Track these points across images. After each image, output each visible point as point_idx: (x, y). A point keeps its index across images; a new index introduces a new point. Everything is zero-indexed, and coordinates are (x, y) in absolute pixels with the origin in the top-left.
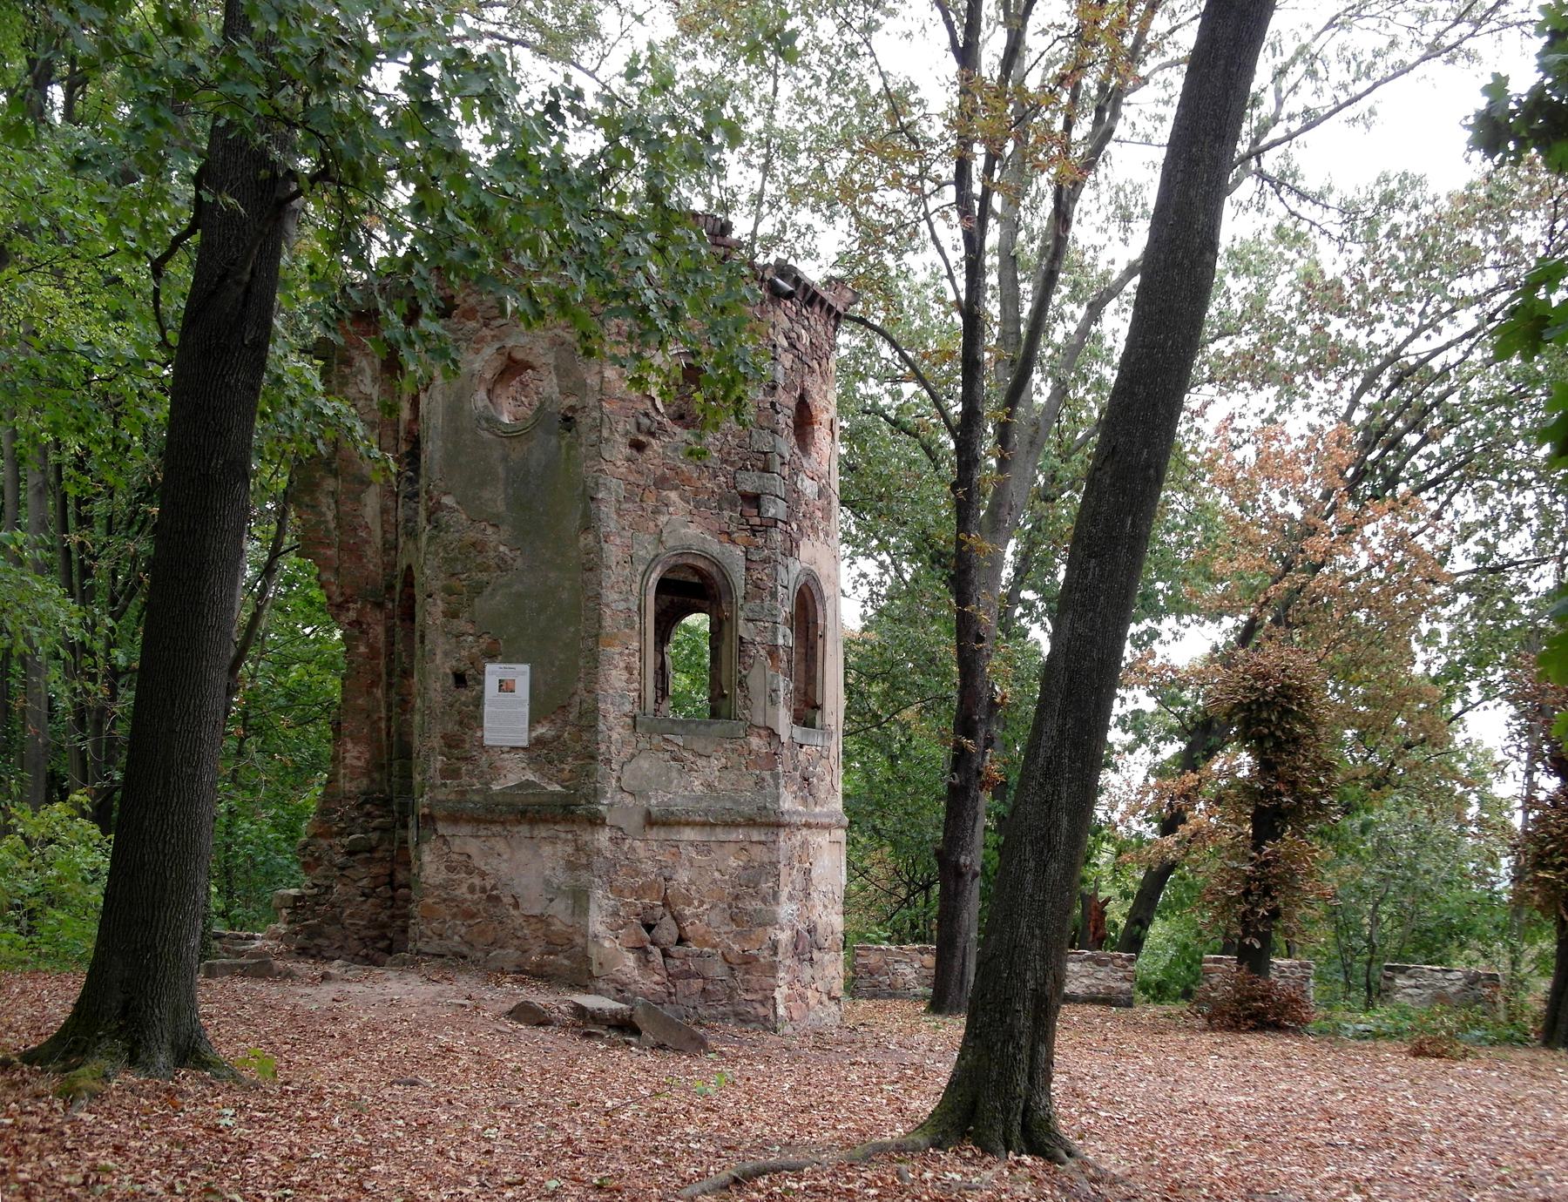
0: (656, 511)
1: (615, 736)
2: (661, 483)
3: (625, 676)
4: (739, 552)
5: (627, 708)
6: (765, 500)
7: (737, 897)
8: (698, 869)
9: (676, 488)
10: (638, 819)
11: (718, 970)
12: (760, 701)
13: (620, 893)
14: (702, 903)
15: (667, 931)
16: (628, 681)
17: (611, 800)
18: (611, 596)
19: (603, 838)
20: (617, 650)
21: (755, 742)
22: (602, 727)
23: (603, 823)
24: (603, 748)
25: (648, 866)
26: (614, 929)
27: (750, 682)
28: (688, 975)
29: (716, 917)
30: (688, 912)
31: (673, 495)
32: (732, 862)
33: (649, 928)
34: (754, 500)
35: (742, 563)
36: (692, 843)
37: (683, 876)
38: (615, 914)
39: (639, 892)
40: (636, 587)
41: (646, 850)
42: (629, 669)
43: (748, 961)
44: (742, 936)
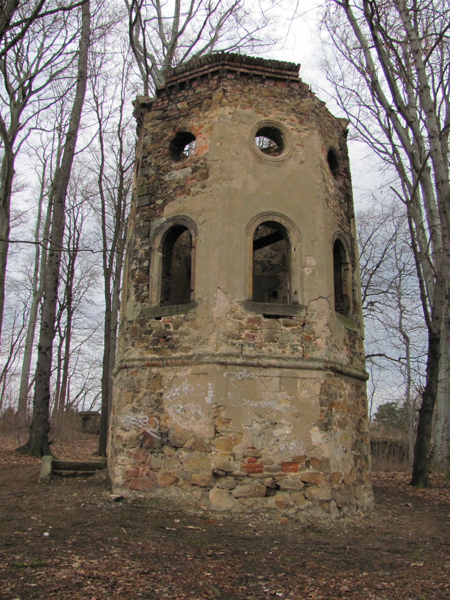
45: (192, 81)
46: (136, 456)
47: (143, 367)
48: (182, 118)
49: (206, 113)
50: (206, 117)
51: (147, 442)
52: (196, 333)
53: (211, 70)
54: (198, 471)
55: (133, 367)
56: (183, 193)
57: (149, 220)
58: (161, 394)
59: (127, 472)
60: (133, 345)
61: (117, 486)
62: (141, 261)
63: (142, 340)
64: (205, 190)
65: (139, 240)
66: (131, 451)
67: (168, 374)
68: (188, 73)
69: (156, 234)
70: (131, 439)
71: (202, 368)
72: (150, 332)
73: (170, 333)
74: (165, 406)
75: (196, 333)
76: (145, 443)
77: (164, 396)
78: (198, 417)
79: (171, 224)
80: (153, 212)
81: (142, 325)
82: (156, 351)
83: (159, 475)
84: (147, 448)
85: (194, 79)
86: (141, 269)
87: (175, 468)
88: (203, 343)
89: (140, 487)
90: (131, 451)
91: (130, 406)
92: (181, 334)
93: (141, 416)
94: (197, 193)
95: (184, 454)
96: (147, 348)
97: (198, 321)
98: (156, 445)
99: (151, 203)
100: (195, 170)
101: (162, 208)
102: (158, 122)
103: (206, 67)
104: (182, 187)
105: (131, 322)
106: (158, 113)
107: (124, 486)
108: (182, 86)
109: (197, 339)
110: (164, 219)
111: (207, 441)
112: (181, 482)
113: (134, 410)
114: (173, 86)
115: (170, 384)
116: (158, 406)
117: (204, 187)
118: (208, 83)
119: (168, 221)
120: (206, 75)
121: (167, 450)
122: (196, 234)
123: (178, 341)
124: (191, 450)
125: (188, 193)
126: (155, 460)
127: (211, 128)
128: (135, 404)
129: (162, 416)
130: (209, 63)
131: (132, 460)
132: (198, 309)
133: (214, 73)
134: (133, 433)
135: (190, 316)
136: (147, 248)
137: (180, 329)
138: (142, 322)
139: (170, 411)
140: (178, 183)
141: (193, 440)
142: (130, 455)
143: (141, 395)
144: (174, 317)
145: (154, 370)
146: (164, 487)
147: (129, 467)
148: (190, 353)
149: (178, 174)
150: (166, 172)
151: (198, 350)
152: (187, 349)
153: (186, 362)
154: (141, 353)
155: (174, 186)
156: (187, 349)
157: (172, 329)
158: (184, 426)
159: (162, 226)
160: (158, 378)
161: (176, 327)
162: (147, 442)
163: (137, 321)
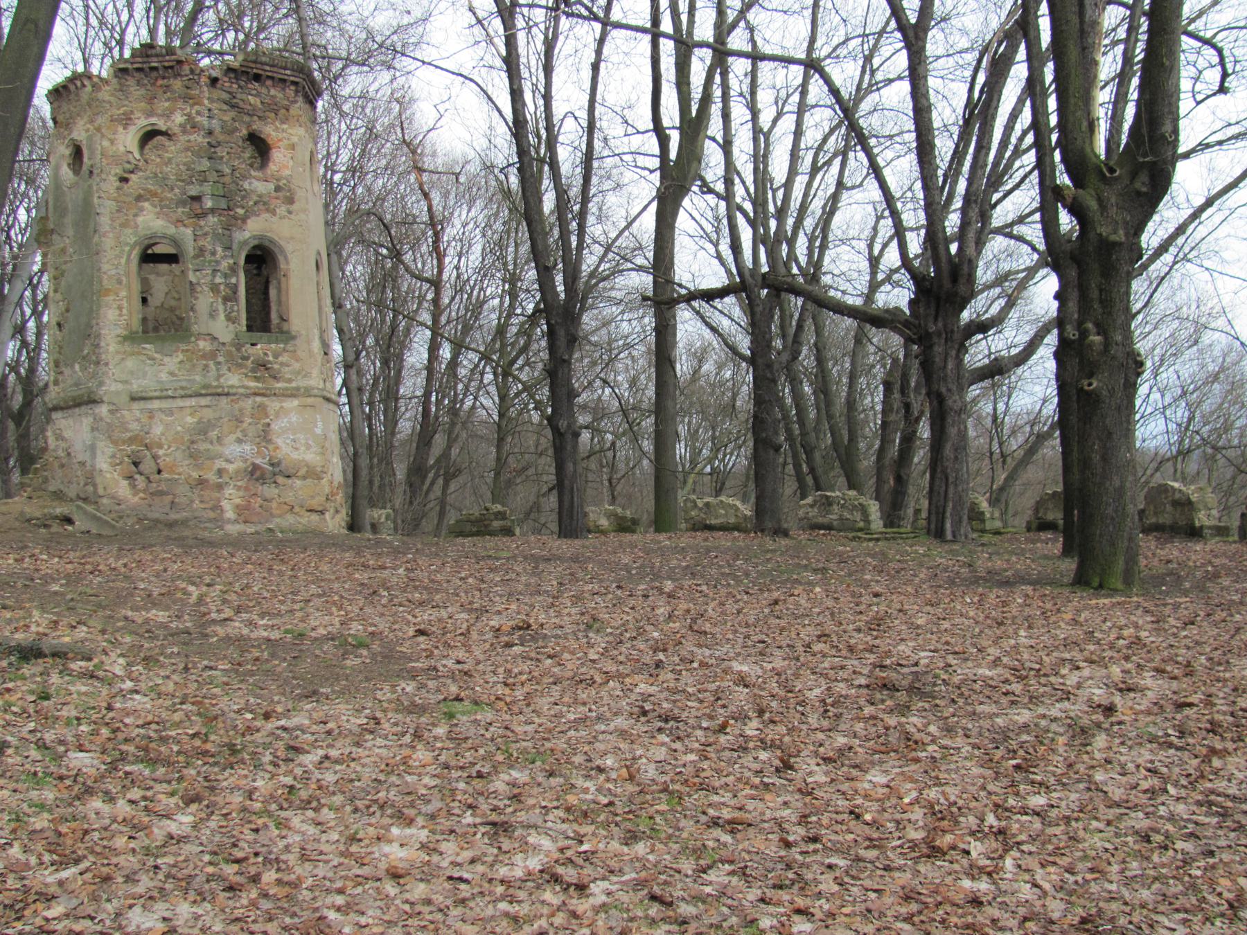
0: (136, 215)
1: (111, 349)
2: (139, 198)
3: (117, 312)
4: (189, 231)
5: (119, 331)
6: (204, 199)
7: (193, 442)
8: (168, 427)
9: (148, 200)
10: (125, 398)
11: (182, 490)
12: (204, 317)
13: (115, 443)
14: (169, 447)
15: (148, 466)
16: (120, 315)
17: (111, 387)
18: (105, 267)
19: (103, 410)
20: (111, 298)
21: (202, 344)
22: (102, 344)
23: (102, 402)
24: (103, 357)
25: (134, 426)
26: (114, 465)
27: (197, 307)
28: (161, 493)
29: (179, 455)
30: (161, 452)
31: (146, 205)
32: (189, 419)
33: (136, 464)
34: (197, 199)
35: (191, 238)
36: (160, 409)
37: (158, 430)
38: (113, 456)
39: (131, 440)
40: (123, 261)
41: (133, 416)
42: (120, 308)
43: (201, 482)
44: (198, 467)
45: (268, 77)
46: (247, 489)
47: (247, 396)
48: (255, 118)
49: (285, 126)
50: (283, 131)
51: (258, 473)
52: (297, 366)
53: (292, 78)
54: (313, 497)
55: (234, 394)
56: (267, 210)
57: (227, 228)
58: (269, 425)
59: (238, 506)
60: (229, 370)
61: (229, 521)
62: (226, 276)
63: (240, 366)
64: (292, 216)
65: (219, 250)
66: (239, 484)
67: (273, 405)
68: (268, 68)
69: (241, 248)
70: (237, 472)
71: (310, 400)
72: (247, 358)
73: (270, 362)
74: (274, 438)
75: (297, 366)
76: (255, 474)
77: (273, 426)
78: (308, 447)
79: (256, 242)
80: (233, 221)
81: (238, 350)
82: (257, 379)
83: (274, 505)
84: (257, 480)
85: (272, 78)
86: (227, 285)
87: (289, 497)
88: (305, 376)
89: (255, 519)
90: (239, 484)
91: (233, 437)
92: (282, 364)
93: (247, 447)
94: (284, 217)
95: (298, 483)
96: (246, 376)
97: (299, 353)
98: (268, 476)
99: (229, 209)
100: (278, 189)
101: (244, 220)
102: (225, 107)
103: (288, 72)
104: (265, 203)
105: (224, 344)
106: (225, 96)
107: (236, 521)
108: (257, 78)
109: (299, 373)
110: (247, 235)
111: (319, 469)
112: (297, 509)
113: (239, 441)
114: (247, 73)
115: (277, 415)
116: (265, 436)
117: (290, 213)
118: (283, 89)
119: (254, 237)
120: (284, 81)
121: (280, 480)
122: (288, 263)
123: (279, 371)
124: (304, 478)
125: (274, 213)
126: (270, 491)
127: (293, 147)
128: (239, 434)
129: (271, 447)
130: (293, 70)
131: (241, 493)
132: (297, 342)
133: (294, 83)
134: (239, 464)
135: (290, 347)
136: (231, 261)
137: (280, 359)
138: (239, 347)
139: (280, 442)
140: (260, 196)
141: (305, 469)
142: (239, 488)
143: (245, 425)
144: (273, 346)
145: (258, 399)
146: (280, 516)
147: (238, 501)
148: (294, 385)
149: (258, 186)
150: (244, 177)
151: (301, 383)
152: (290, 381)
153: (293, 394)
154: (240, 380)
155: (255, 198)
156: (290, 381)
157: (271, 358)
158: (295, 456)
159: (245, 242)
160: (262, 408)
161: (276, 356)
162: (258, 473)
163: (233, 345)
